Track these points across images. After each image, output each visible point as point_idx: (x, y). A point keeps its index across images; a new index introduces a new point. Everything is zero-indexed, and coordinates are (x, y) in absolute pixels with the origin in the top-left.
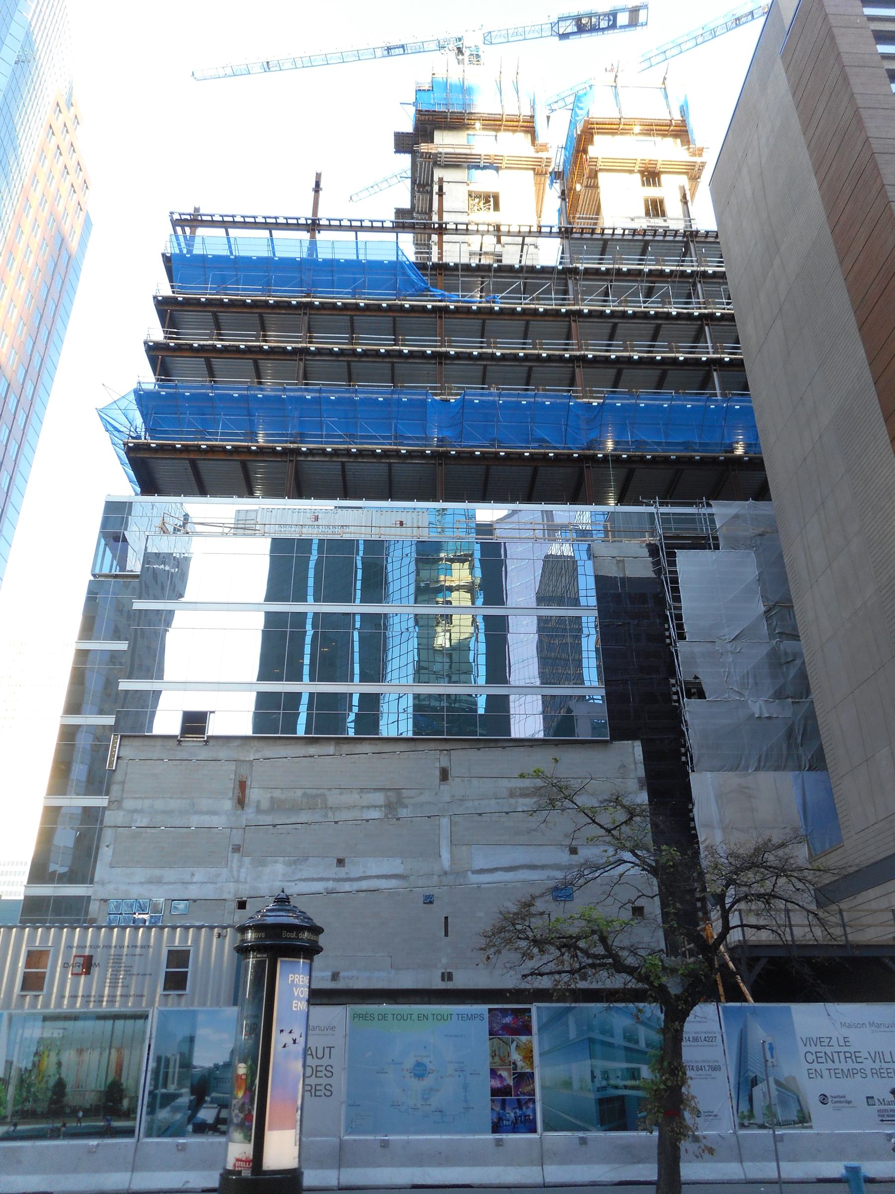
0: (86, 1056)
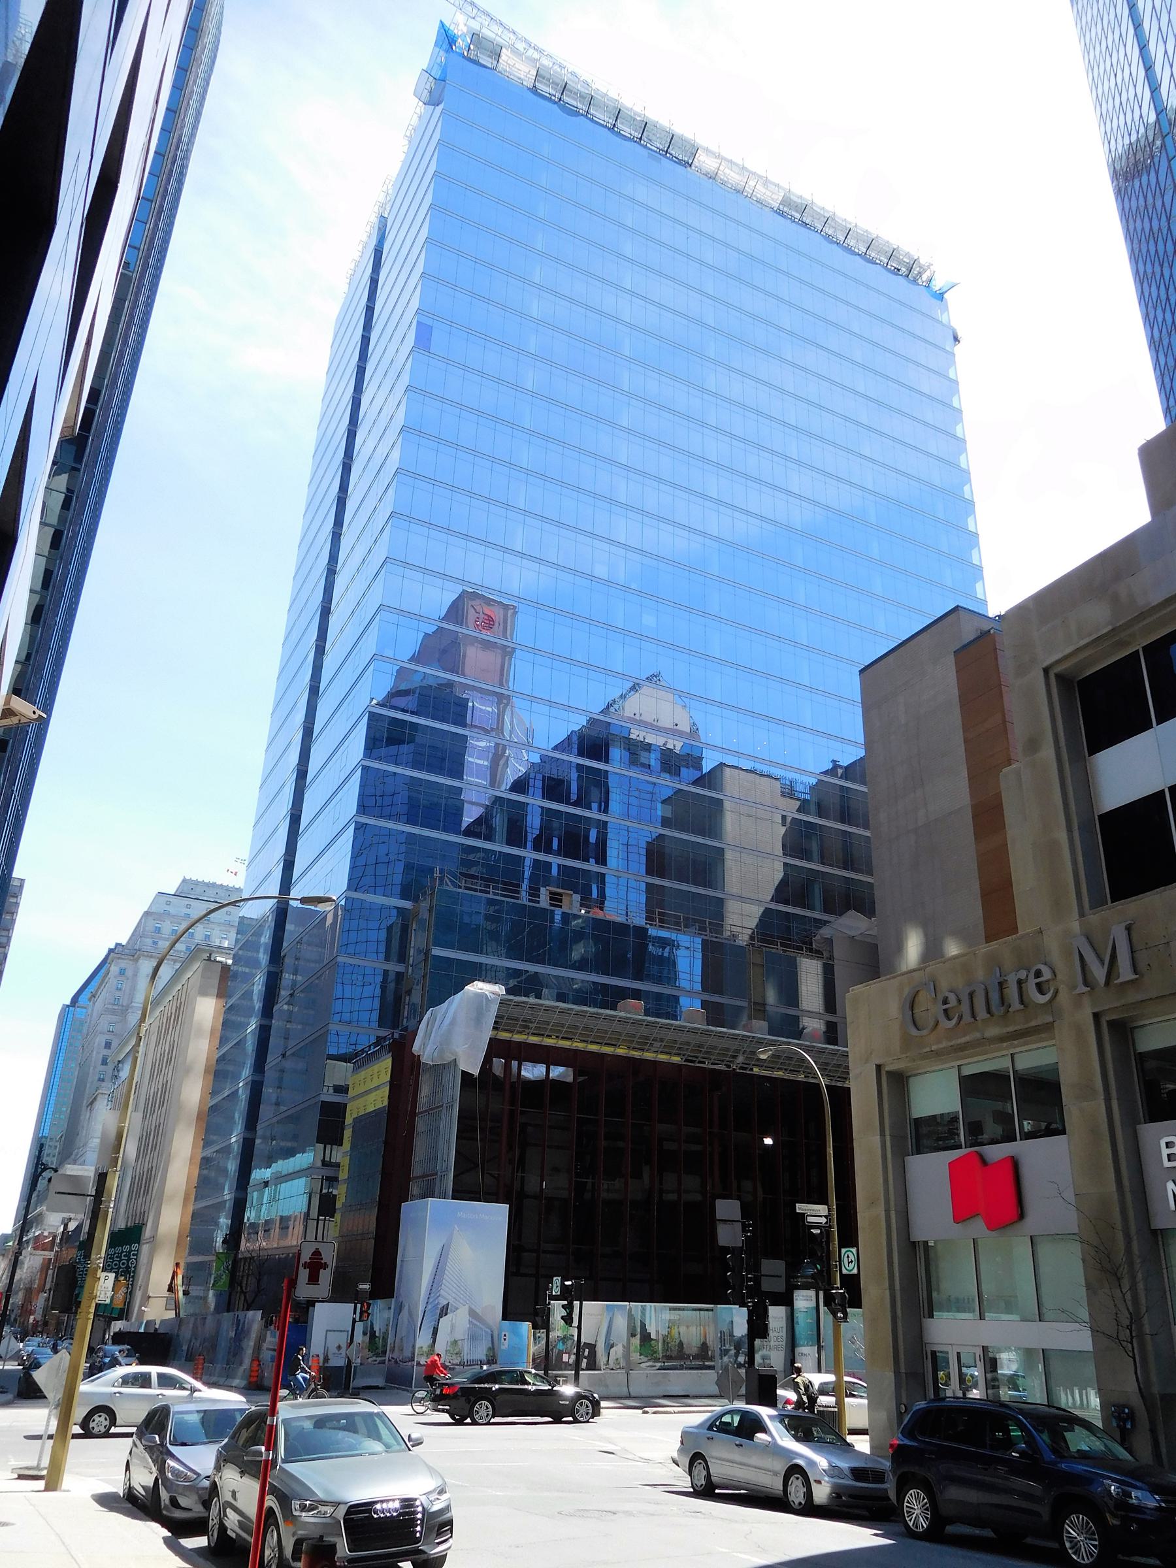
0: (690, 1328)
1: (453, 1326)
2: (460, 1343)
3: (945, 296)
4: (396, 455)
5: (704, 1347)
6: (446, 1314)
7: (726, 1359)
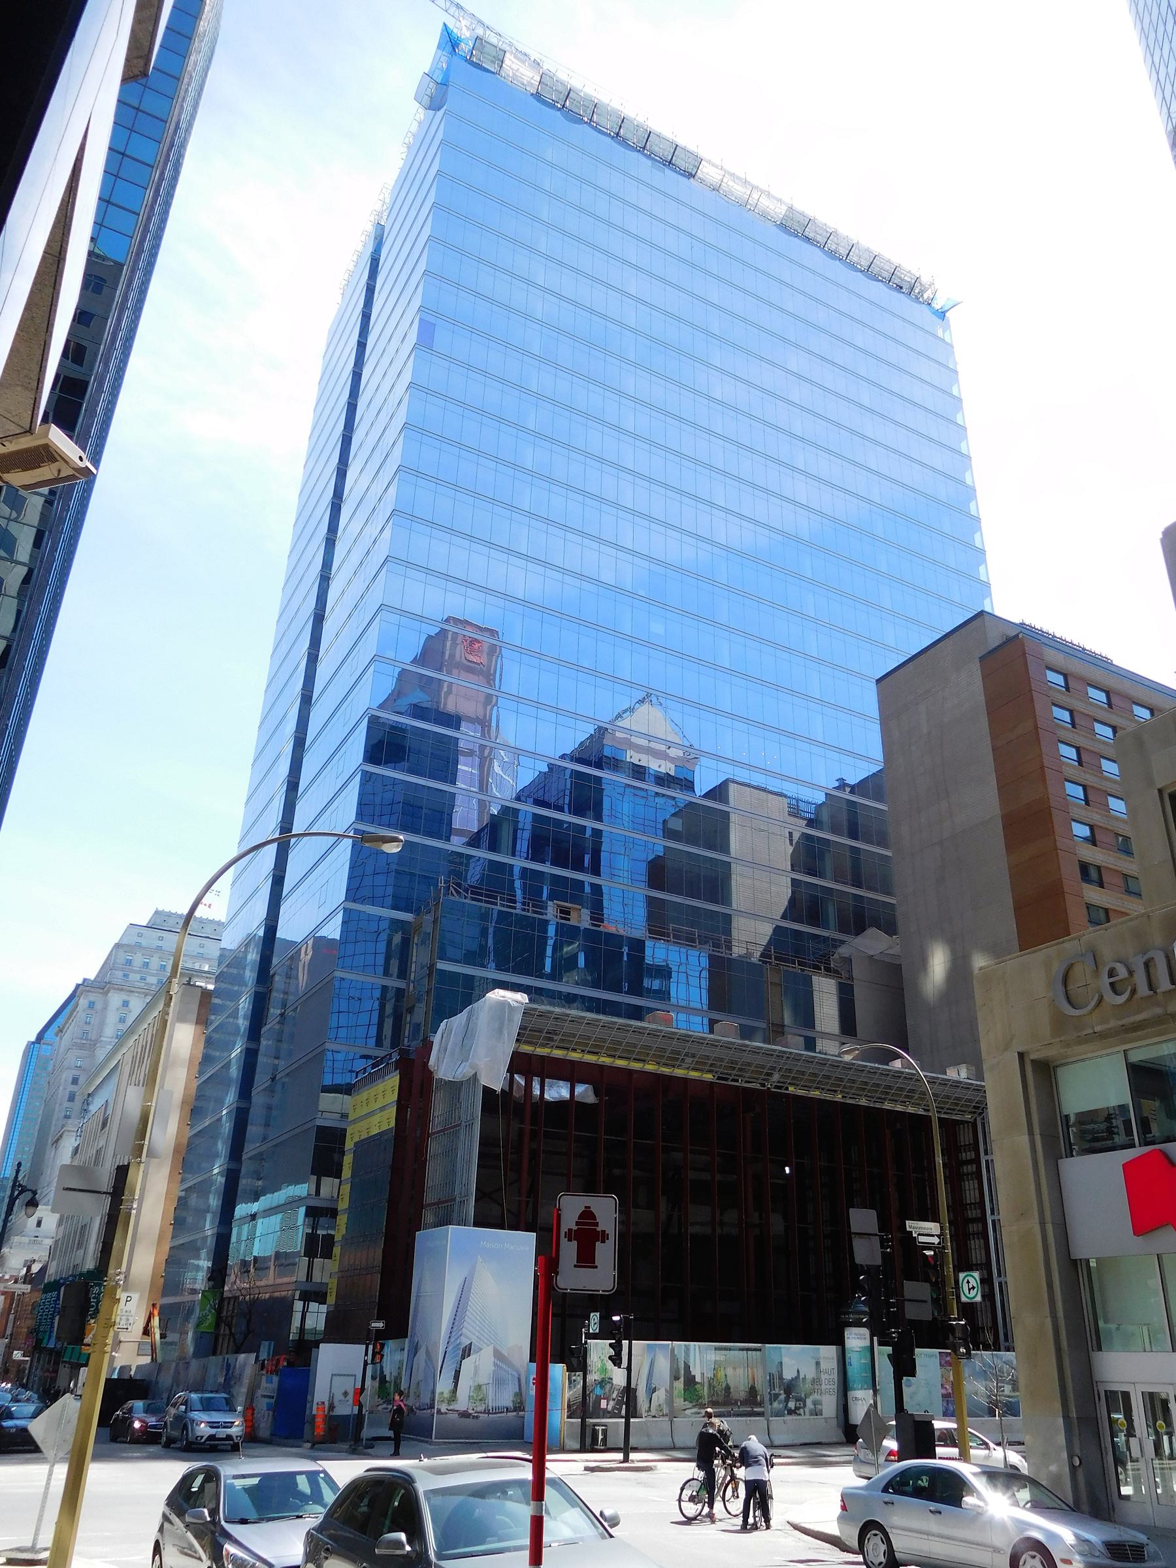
1: (476, 1369)
2: (484, 1388)
3: (947, 314)
4: (397, 452)
5: (753, 1391)
6: (469, 1356)
7: (775, 1404)
